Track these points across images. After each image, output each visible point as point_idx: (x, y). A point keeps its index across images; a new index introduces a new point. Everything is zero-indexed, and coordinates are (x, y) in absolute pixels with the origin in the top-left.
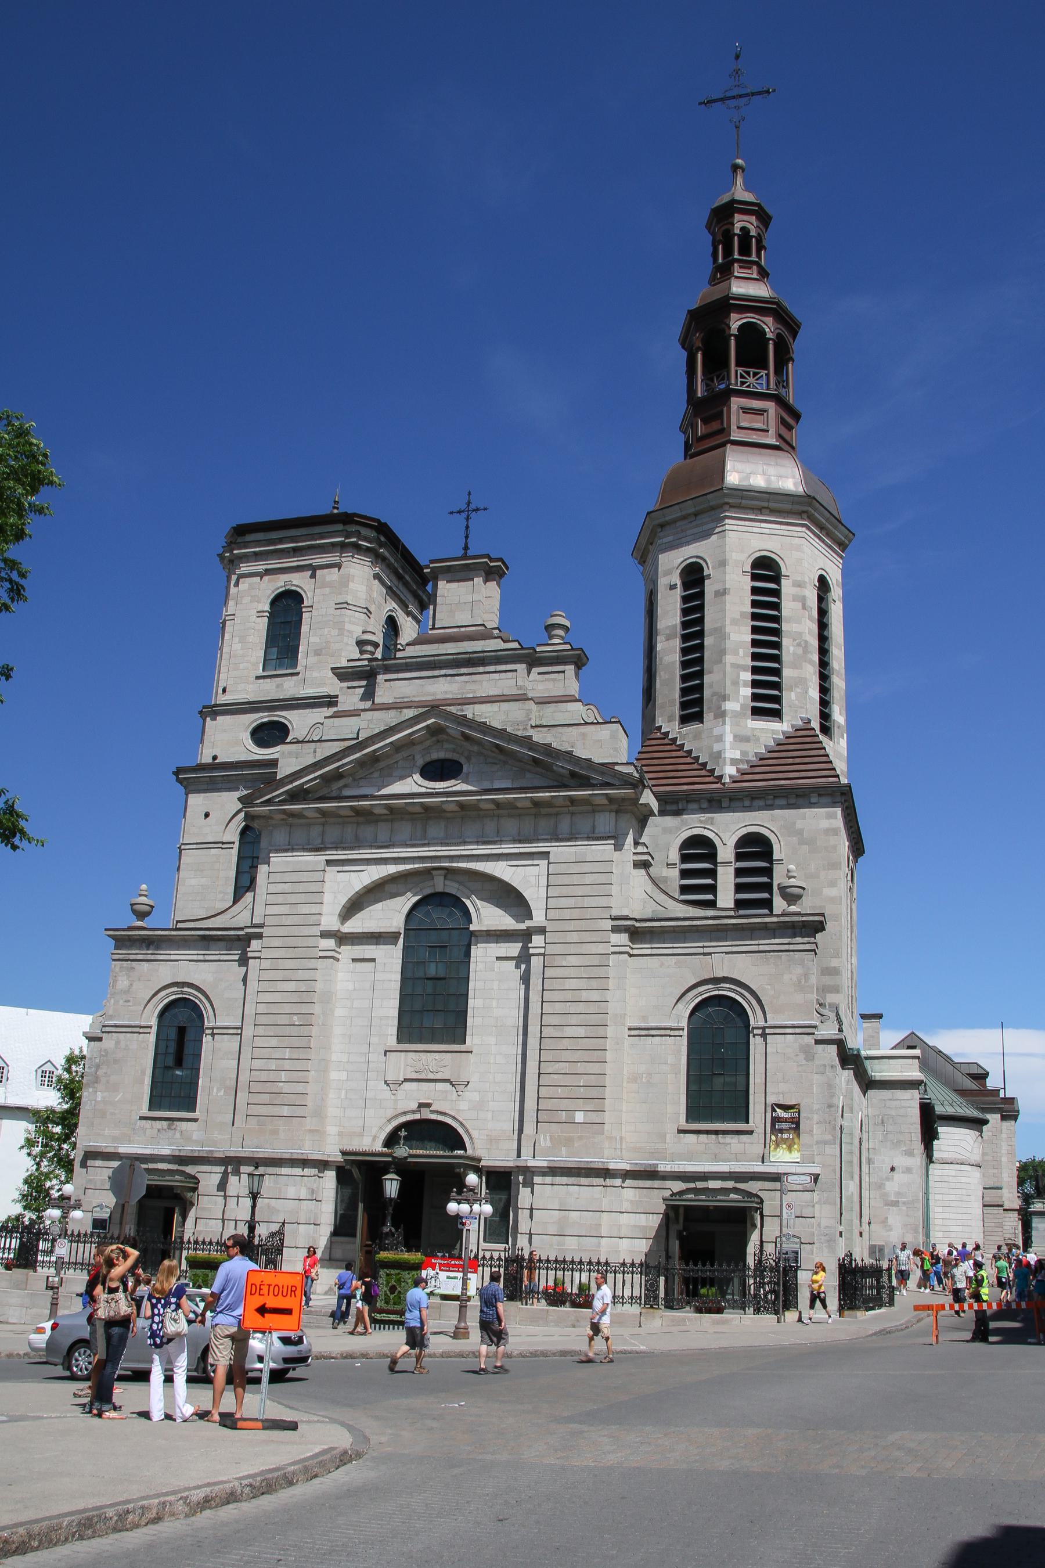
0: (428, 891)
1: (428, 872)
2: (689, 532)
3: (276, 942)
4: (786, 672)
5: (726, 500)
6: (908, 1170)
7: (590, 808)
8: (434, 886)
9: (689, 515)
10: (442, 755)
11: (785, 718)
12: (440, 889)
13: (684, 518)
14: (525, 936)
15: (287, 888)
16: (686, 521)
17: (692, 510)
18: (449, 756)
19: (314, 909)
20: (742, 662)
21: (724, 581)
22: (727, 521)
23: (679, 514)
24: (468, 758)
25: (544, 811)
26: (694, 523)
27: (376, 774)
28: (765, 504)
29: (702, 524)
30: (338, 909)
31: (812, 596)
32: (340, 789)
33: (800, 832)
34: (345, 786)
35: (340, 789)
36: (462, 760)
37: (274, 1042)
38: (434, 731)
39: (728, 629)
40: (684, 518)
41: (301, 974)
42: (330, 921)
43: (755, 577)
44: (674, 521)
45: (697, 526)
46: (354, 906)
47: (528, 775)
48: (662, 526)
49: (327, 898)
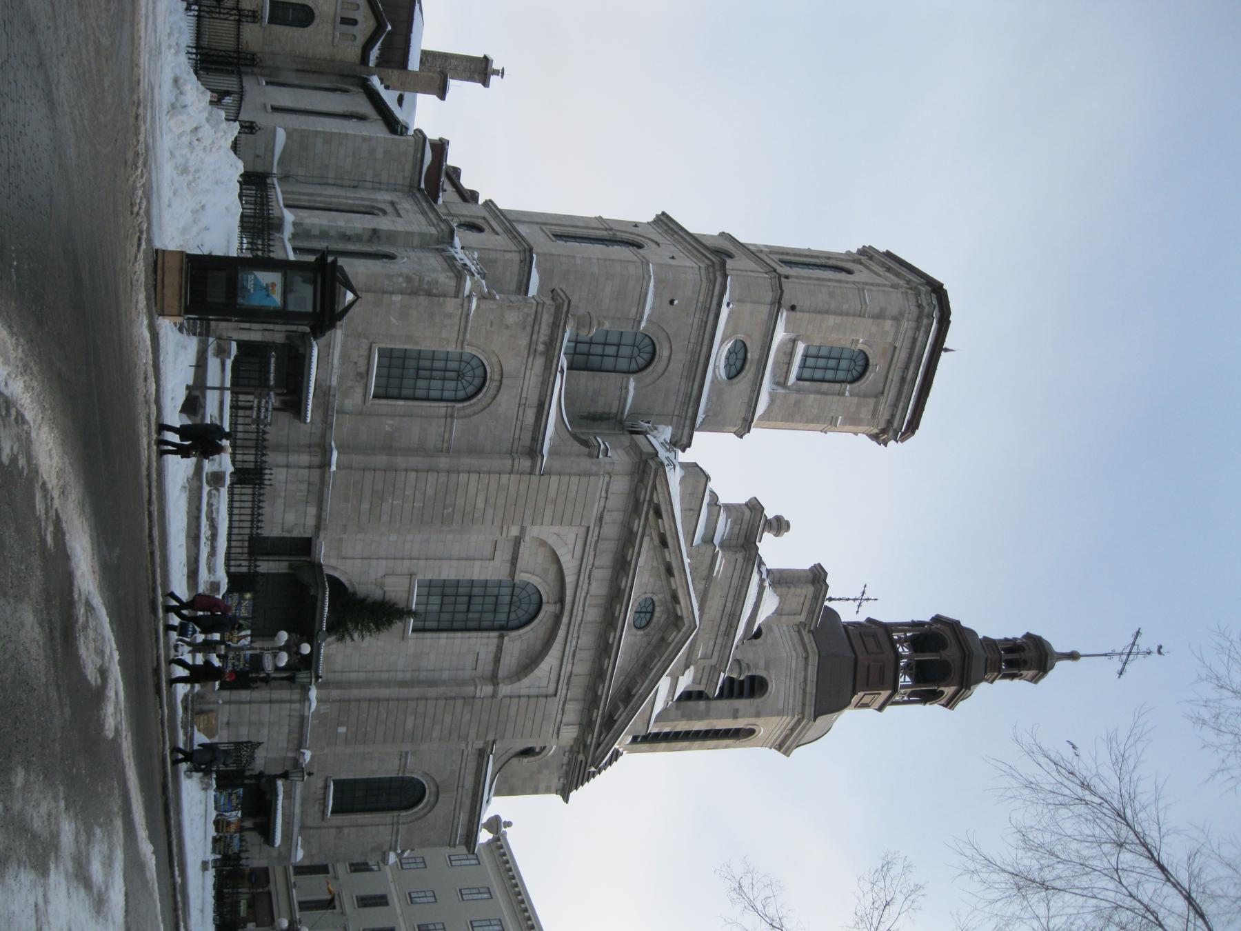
1: (561, 600)
2: (793, 683)
3: (523, 488)
4: (663, 745)
5: (805, 720)
7: (584, 723)
8: (548, 603)
9: (806, 685)
10: (657, 614)
11: (630, 746)
12: (545, 608)
13: (805, 680)
14: (494, 679)
15: (572, 495)
16: (802, 680)
17: (808, 690)
18: (655, 619)
19: (547, 519)
21: (743, 717)
22: (789, 718)
23: (809, 679)
24: (646, 635)
26: (798, 686)
27: (655, 564)
28: (794, 735)
29: (795, 696)
30: (543, 537)
32: (651, 535)
33: (540, 772)
34: (652, 539)
35: (651, 535)
36: (648, 629)
37: (430, 492)
38: (676, 621)
39: (706, 722)
40: (805, 680)
41: (490, 512)
42: (534, 531)
44: (806, 670)
45: (795, 691)
46: (543, 543)
47: (622, 678)
48: (806, 659)
49: (556, 529)
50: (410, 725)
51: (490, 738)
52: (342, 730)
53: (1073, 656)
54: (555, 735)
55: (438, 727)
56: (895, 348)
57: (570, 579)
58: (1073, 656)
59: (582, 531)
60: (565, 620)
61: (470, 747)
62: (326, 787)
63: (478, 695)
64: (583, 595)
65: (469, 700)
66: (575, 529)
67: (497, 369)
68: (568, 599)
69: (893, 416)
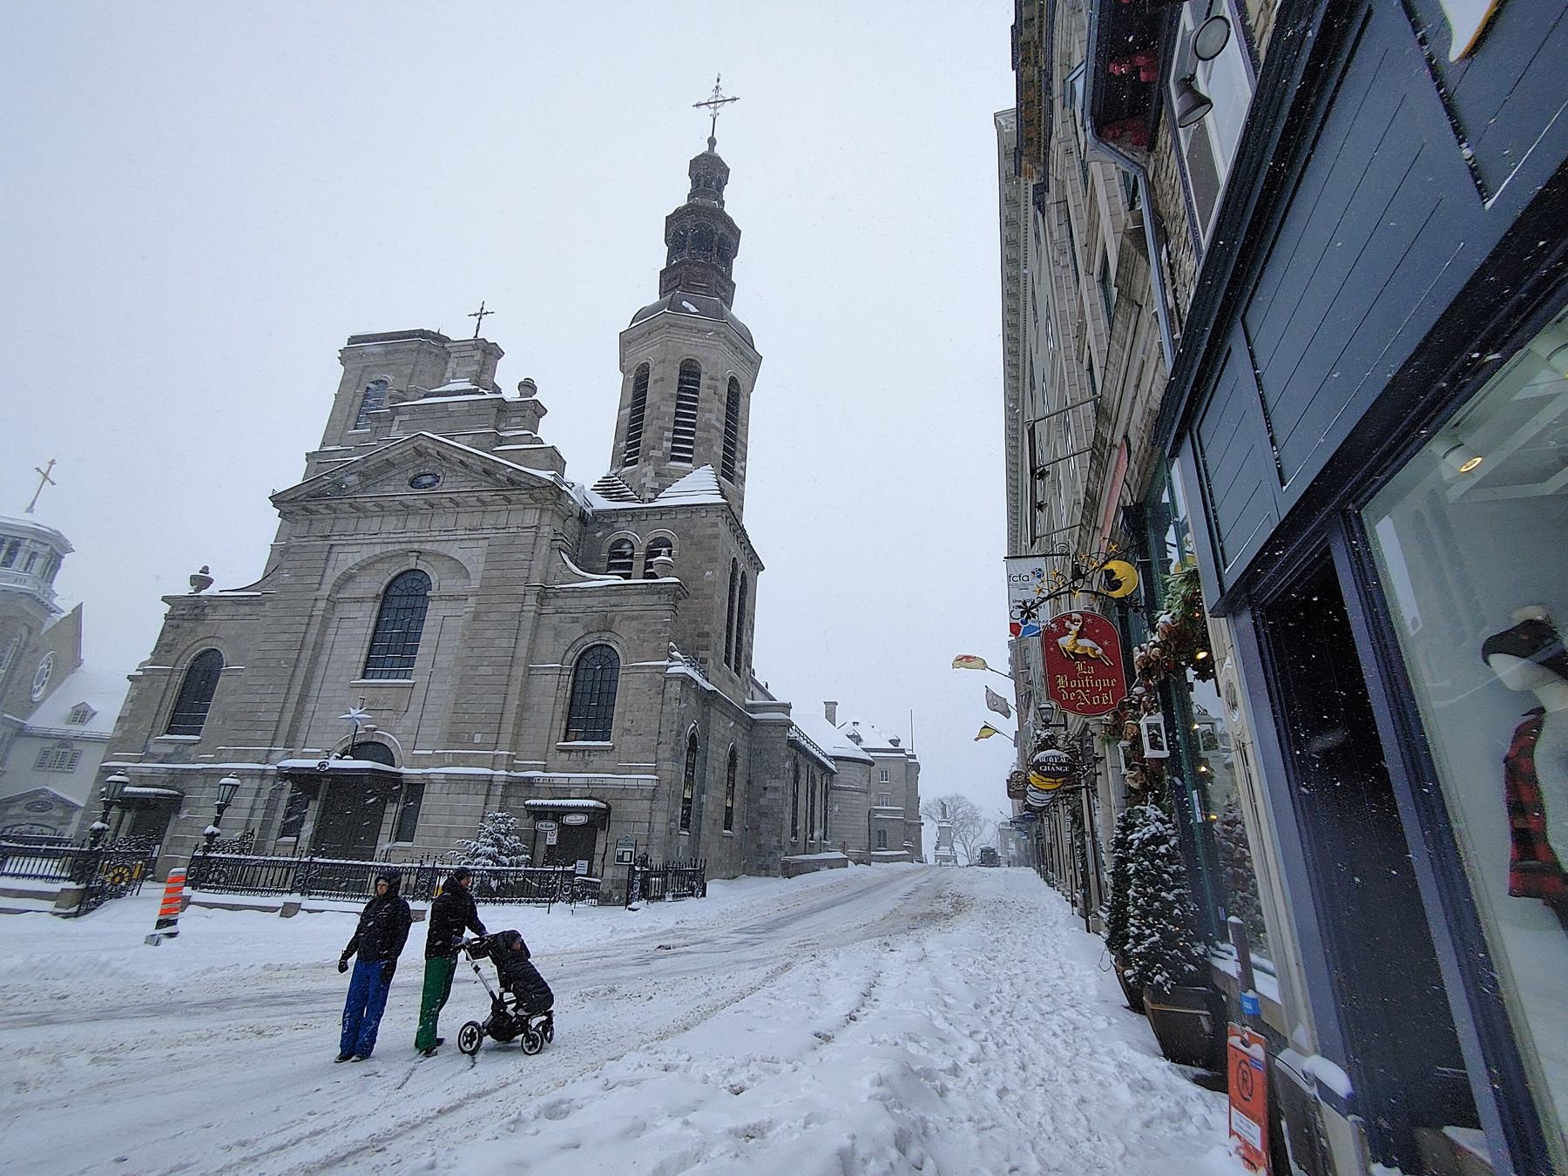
0: (404, 569)
6: (776, 789)
12: (413, 567)
20: (667, 425)
25: (490, 508)
31: (724, 389)
37: (262, 681)
43: (682, 373)
46: (348, 578)
49: (329, 571)
50: (490, 670)
51: (521, 589)
52: (478, 738)
53: (712, 142)
54: (533, 529)
55: (497, 641)
56: (366, 367)
57: (378, 550)
58: (712, 142)
59: (335, 549)
60: (416, 546)
61: (530, 608)
62: (569, 751)
63: (473, 609)
64: (392, 536)
65: (476, 617)
66: (333, 556)
67: (204, 641)
68: (397, 547)
69: (410, 350)
